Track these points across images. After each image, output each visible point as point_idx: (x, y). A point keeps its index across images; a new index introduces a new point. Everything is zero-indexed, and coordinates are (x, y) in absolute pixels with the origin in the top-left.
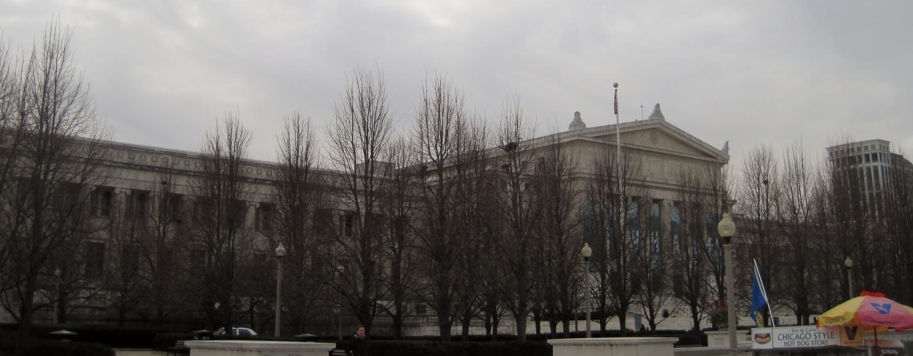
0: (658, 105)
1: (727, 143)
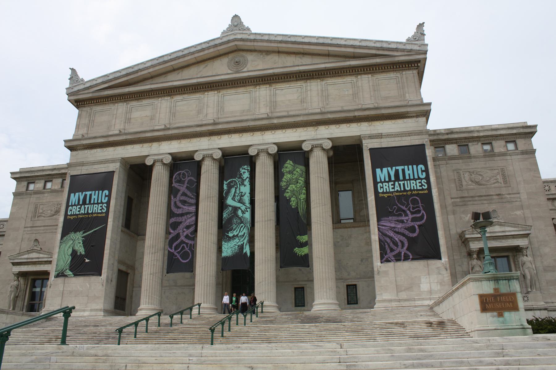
0: (236, 17)
1: (421, 26)
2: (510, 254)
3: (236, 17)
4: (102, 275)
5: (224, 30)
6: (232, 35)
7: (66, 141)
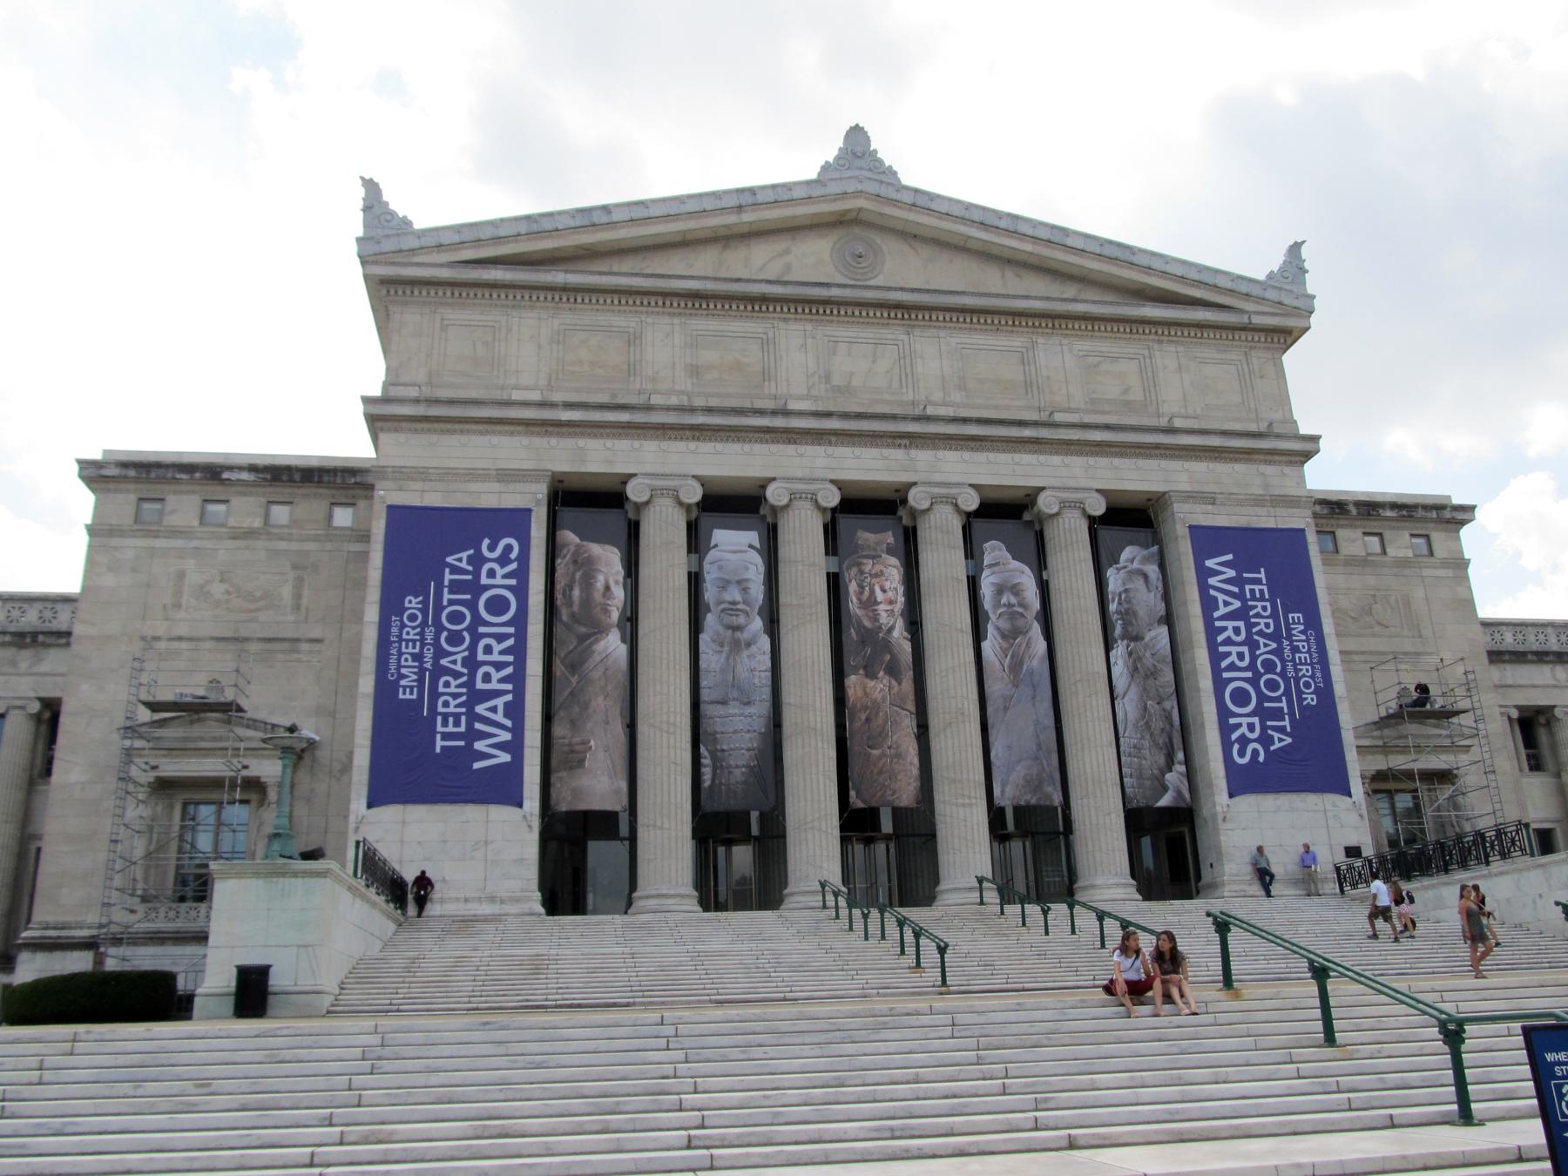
0: (856, 134)
1: (1295, 248)
3: (856, 134)
4: (526, 804)
7: (367, 400)
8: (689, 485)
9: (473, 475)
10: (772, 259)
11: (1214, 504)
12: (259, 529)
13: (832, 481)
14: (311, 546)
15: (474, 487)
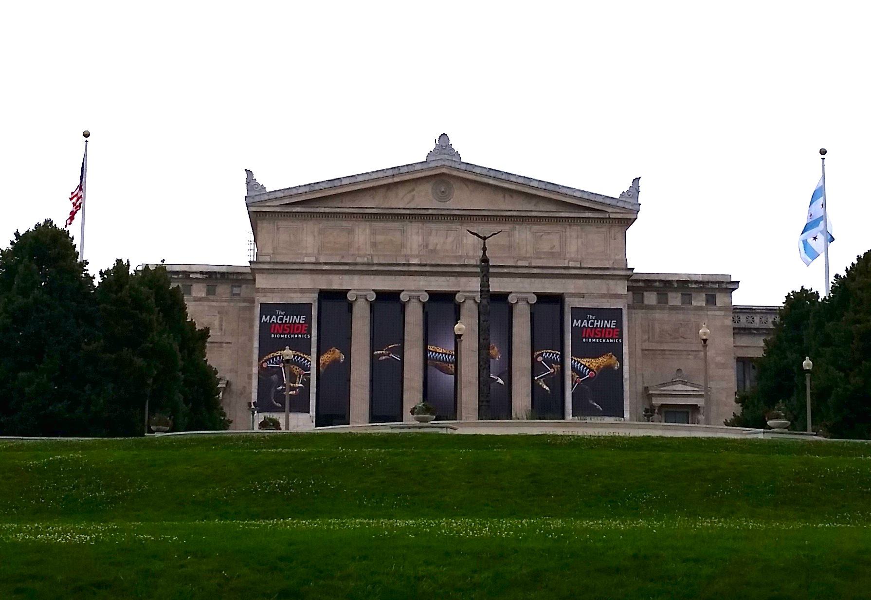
2: (690, 411)
5: (431, 151)
6: (440, 161)
8: (371, 294)
9: (290, 290)
10: (408, 193)
11: (584, 298)
12: (204, 297)
13: (426, 291)
14: (225, 304)
15: (292, 295)
